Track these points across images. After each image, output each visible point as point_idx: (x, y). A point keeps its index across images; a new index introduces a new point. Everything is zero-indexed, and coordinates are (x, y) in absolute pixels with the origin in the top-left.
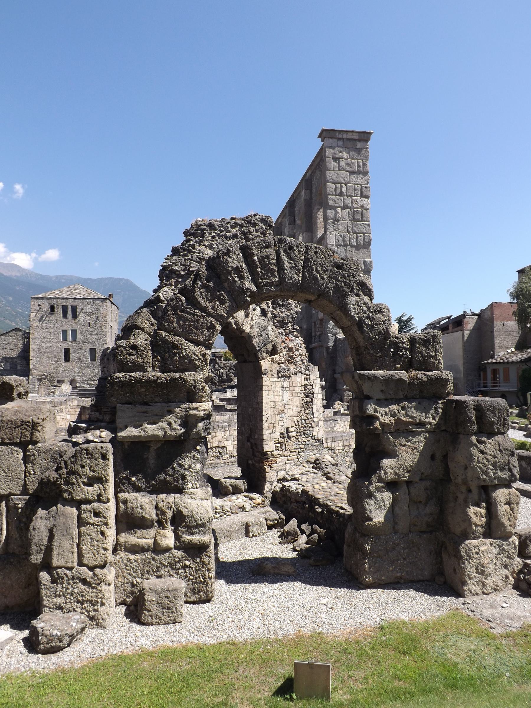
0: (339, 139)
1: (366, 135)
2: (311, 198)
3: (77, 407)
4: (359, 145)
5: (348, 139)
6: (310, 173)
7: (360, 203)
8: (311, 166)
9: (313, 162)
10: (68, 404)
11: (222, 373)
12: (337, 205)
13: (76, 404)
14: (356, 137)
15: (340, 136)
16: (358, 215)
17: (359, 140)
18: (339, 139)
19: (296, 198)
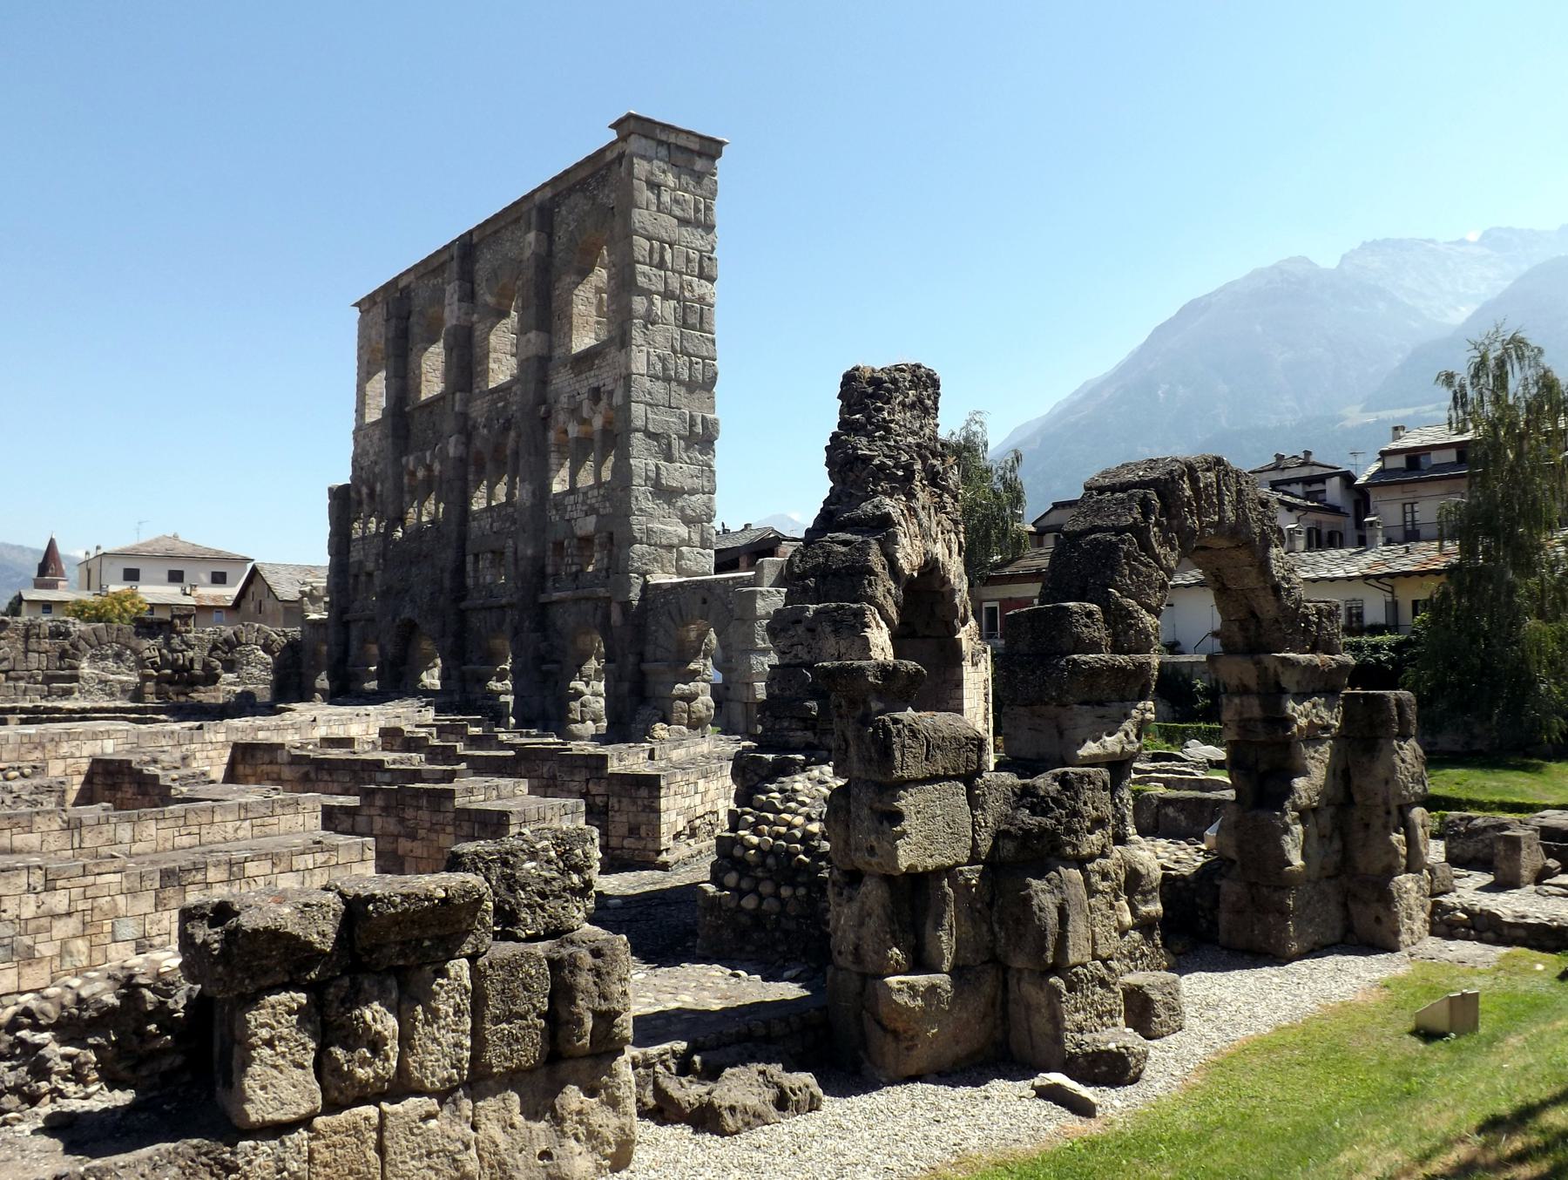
0: (661, 143)
1: (714, 146)
2: (550, 254)
3: (224, 744)
4: (699, 164)
5: (678, 147)
6: (548, 193)
7: (698, 292)
8: (555, 179)
9: (566, 172)
10: (207, 737)
11: (192, 660)
12: (653, 288)
13: (221, 737)
14: (694, 145)
15: (664, 137)
16: (695, 317)
17: (700, 154)
18: (661, 143)
19: (481, 241)
